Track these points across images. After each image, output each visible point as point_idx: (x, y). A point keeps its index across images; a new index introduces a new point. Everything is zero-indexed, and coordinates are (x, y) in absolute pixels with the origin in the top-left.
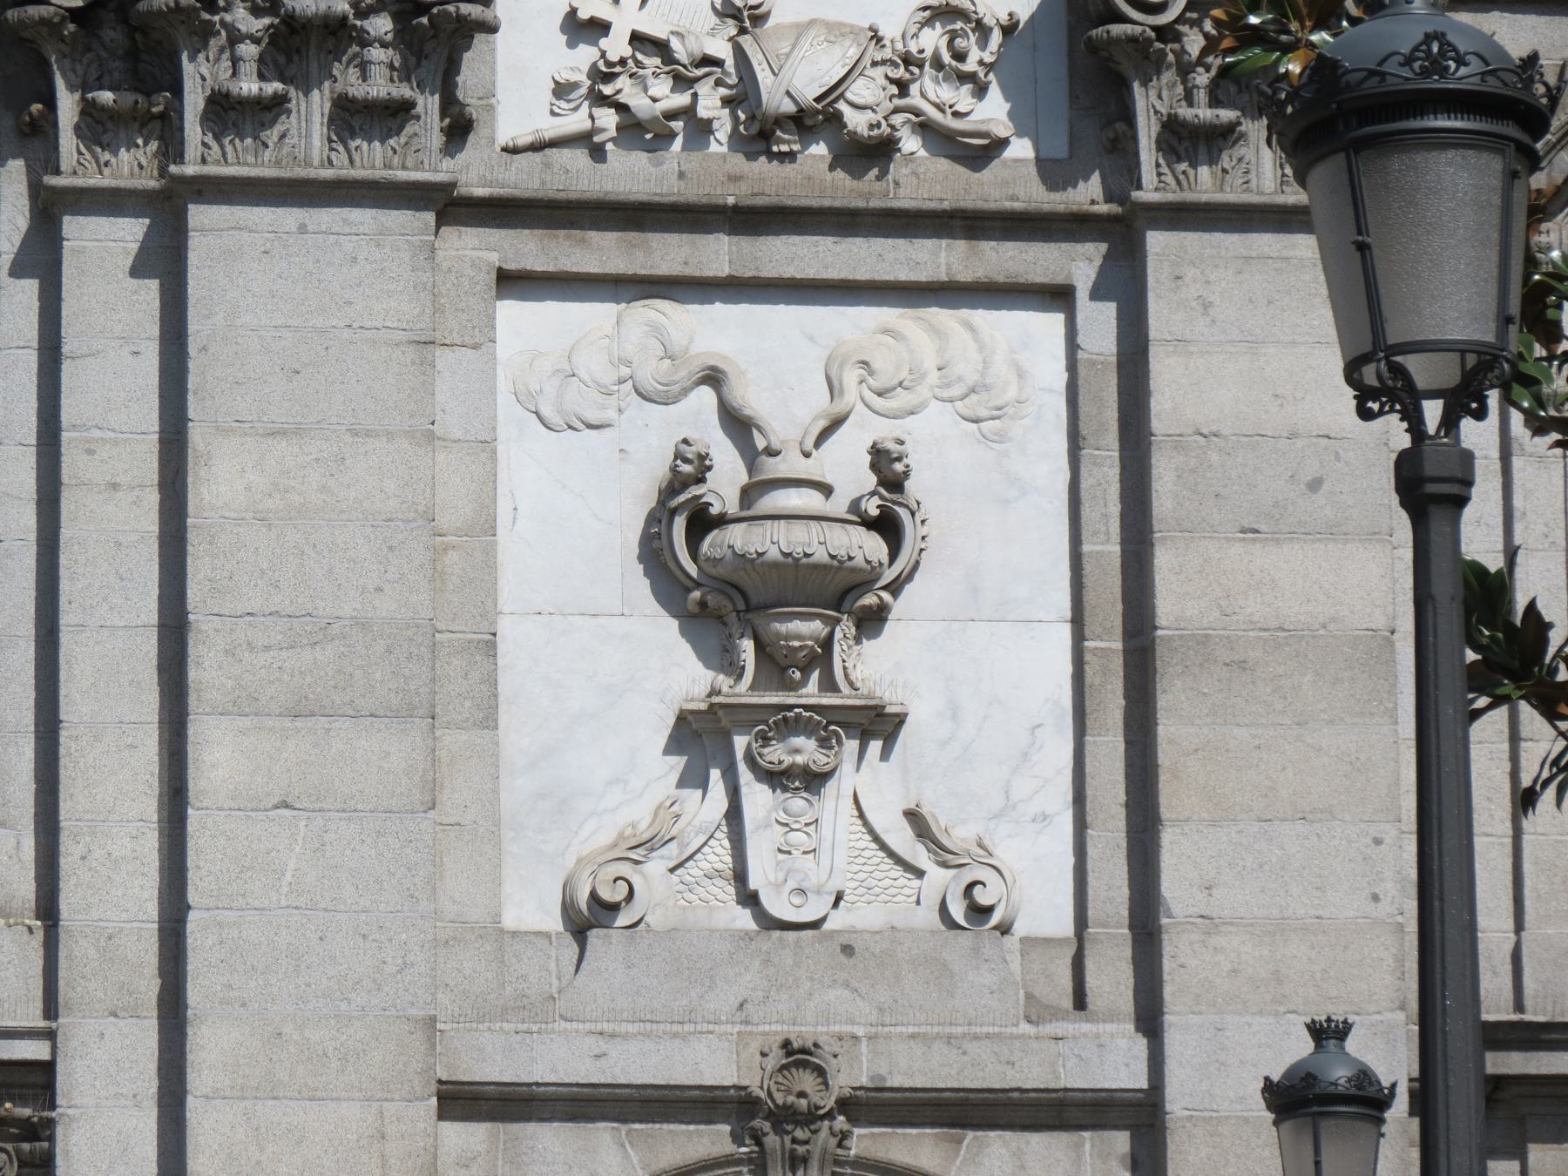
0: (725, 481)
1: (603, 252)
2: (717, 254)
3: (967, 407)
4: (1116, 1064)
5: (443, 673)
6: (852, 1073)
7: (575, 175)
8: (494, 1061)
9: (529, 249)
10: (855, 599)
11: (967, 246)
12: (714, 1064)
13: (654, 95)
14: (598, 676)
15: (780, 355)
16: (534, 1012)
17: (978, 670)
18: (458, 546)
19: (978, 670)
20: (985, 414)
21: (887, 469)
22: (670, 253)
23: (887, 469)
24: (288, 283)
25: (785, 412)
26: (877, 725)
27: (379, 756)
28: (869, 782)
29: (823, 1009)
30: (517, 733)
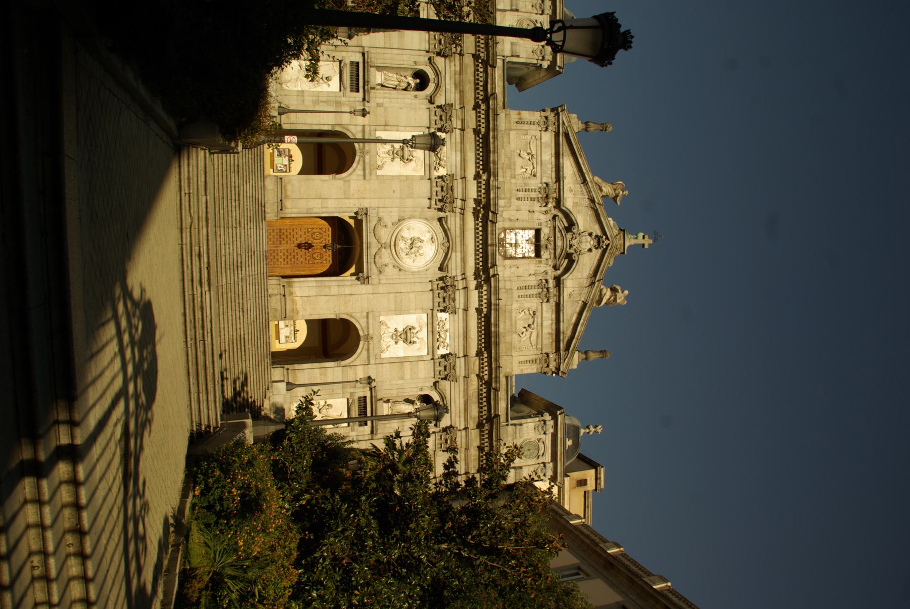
0: (415, 331)
1: (430, 321)
2: (430, 329)
3: (420, 348)
4: (372, 361)
5: (399, 311)
6: (371, 342)
7: (435, 319)
8: (370, 316)
9: (430, 315)
10: (405, 341)
11: (432, 349)
12: (371, 332)
13: (441, 324)
14: (399, 322)
15: (423, 334)
16: (374, 318)
17: (400, 350)
18: (407, 312)
19: (400, 350)
20: (419, 349)
21: (414, 342)
22: (430, 326)
23: (414, 342)
24: (427, 300)
25: (419, 335)
26: (396, 343)
27: (392, 307)
28: (393, 342)
29: (375, 340)
30: (395, 317)
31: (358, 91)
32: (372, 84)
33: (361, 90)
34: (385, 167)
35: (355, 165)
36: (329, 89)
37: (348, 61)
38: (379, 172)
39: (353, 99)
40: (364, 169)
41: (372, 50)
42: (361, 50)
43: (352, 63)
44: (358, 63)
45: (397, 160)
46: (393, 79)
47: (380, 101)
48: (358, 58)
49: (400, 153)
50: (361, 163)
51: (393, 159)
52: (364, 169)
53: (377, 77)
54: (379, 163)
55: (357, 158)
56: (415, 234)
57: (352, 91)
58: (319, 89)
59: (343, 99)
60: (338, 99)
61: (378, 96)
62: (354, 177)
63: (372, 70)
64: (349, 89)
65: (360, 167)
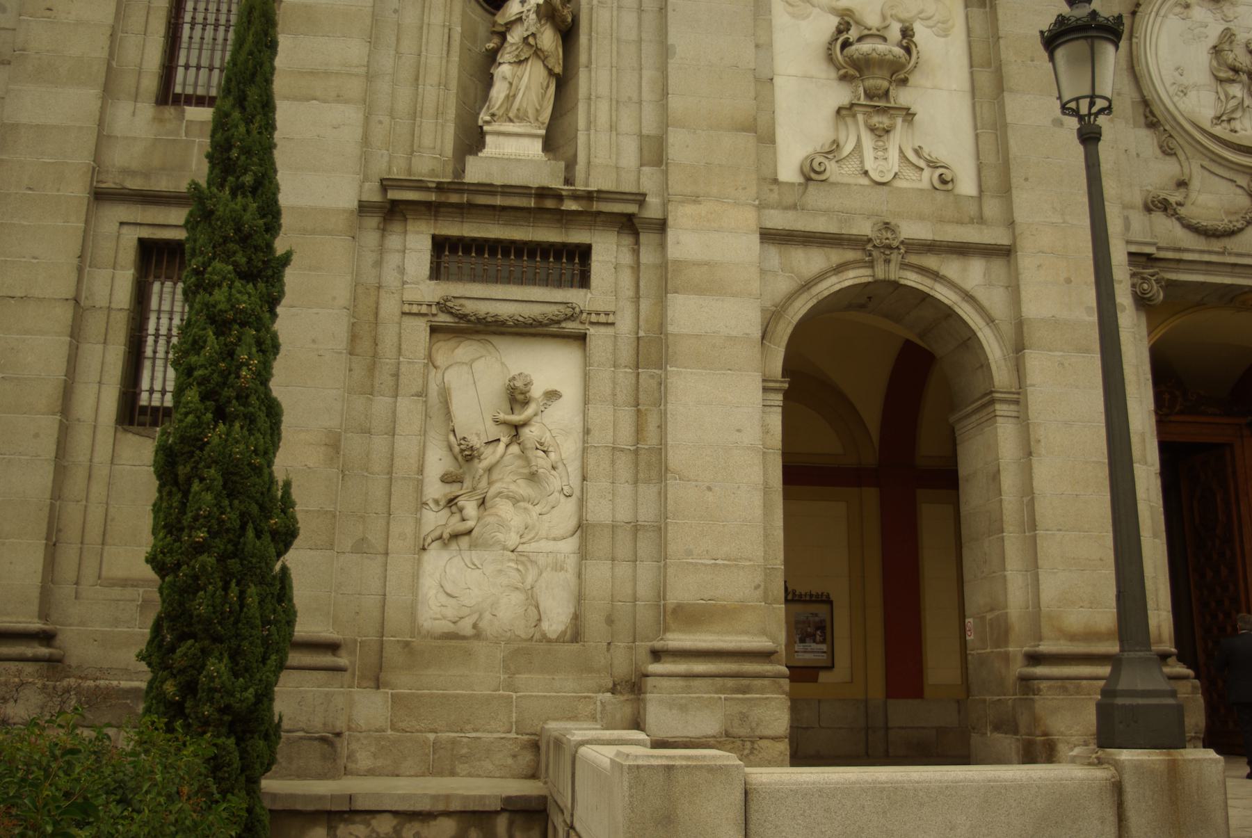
31: (584, 252)
32: (547, 175)
33: (577, 237)
34: (940, 153)
35: (943, 293)
36: (571, 392)
37: (433, 291)
38: (967, 186)
39: (626, 279)
40: (962, 250)
41: (380, 167)
42: (373, 222)
43: (436, 273)
44: (440, 245)
45: (903, 97)
46: (521, 83)
47: (629, 155)
48: (415, 245)
49: (878, 82)
50: (931, 262)
51: (909, 115)
52: (962, 250)
53: (514, 154)
54: (927, 177)
55: (912, 279)
56: (1199, 62)
57: (584, 281)
58: (569, 448)
59: (625, 324)
60: (626, 353)
61: (607, 159)
62: (996, 300)
63: (475, 171)
64: (574, 296)
65: (951, 268)
